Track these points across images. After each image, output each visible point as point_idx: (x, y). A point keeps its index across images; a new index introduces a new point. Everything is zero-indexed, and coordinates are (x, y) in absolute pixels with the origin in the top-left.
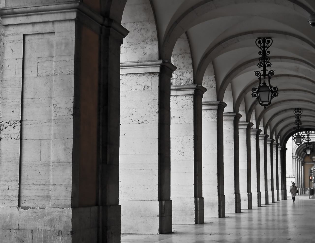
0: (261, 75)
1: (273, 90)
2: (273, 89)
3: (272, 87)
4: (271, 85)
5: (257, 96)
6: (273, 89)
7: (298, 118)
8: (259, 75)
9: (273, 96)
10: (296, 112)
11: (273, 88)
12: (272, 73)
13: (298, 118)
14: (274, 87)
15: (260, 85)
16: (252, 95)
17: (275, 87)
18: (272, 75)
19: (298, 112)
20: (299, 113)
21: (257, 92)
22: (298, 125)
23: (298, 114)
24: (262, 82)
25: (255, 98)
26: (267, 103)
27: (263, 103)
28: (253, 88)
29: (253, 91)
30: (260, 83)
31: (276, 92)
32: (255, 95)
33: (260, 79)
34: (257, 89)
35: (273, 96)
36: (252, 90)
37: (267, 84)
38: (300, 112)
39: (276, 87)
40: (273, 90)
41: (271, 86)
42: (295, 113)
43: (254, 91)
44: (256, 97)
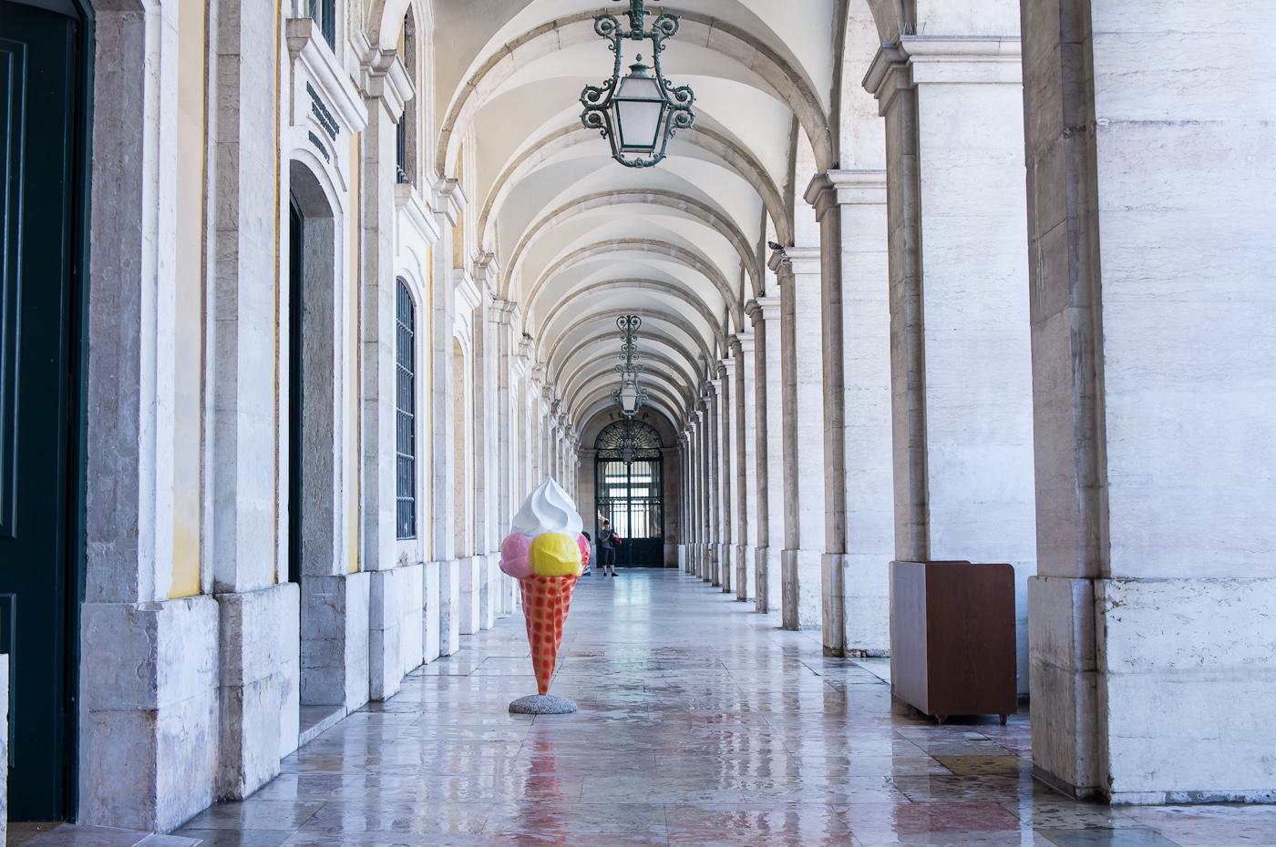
0: (619, 35)
1: (675, 102)
2: (671, 96)
3: (671, 87)
4: (665, 76)
5: (605, 125)
6: (671, 96)
7: (629, 341)
8: (614, 32)
9: (672, 125)
10: (622, 322)
11: (674, 91)
12: (667, 27)
13: (629, 341)
14: (675, 85)
15: (616, 76)
16: (583, 117)
17: (682, 88)
18: (668, 35)
19: (629, 321)
20: (632, 326)
21: (603, 108)
22: (629, 359)
23: (629, 329)
24: (628, 60)
25: (598, 130)
26: (645, 158)
27: (630, 157)
28: (588, 88)
29: (585, 103)
30: (616, 70)
31: (686, 109)
32: (598, 118)
33: (616, 48)
34: (600, 91)
35: (672, 125)
36: (585, 92)
37: (650, 73)
38: (635, 322)
39: (687, 88)
40: (675, 102)
41: (663, 85)
42: (621, 327)
43: (590, 102)
44: (602, 129)
